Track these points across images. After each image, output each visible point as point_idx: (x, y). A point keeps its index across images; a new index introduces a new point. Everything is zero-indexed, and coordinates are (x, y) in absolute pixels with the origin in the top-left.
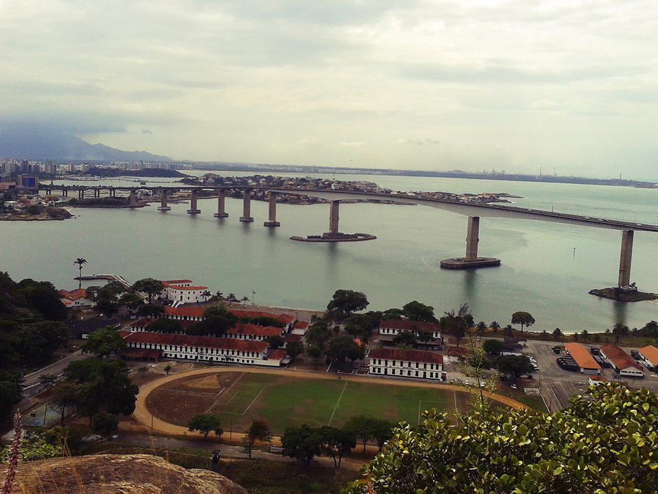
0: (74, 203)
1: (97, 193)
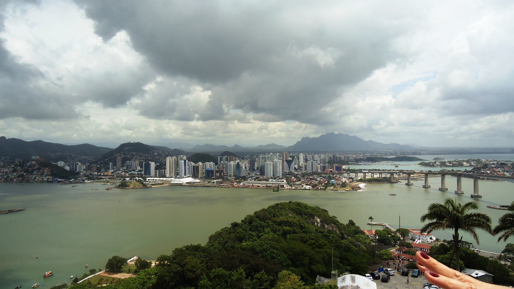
0: (361, 181)
1: (381, 175)
